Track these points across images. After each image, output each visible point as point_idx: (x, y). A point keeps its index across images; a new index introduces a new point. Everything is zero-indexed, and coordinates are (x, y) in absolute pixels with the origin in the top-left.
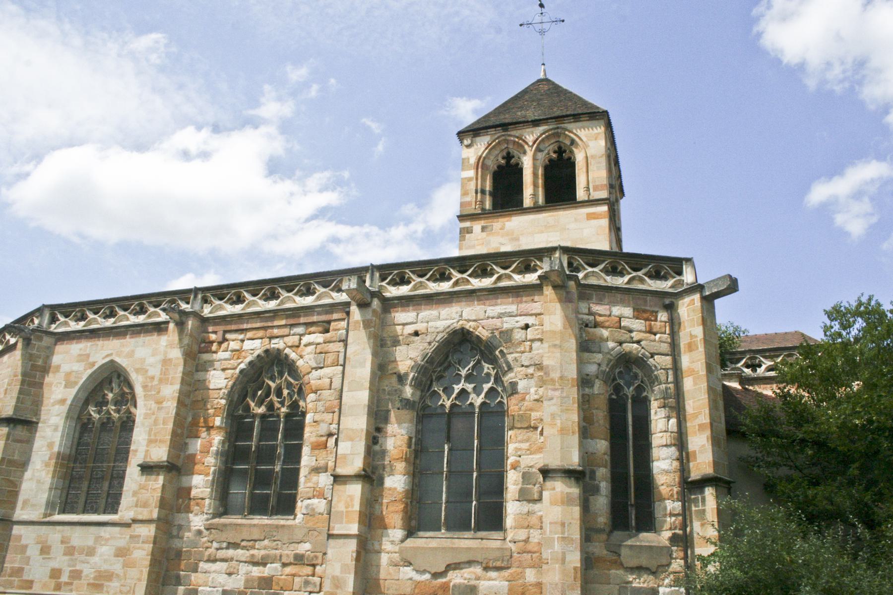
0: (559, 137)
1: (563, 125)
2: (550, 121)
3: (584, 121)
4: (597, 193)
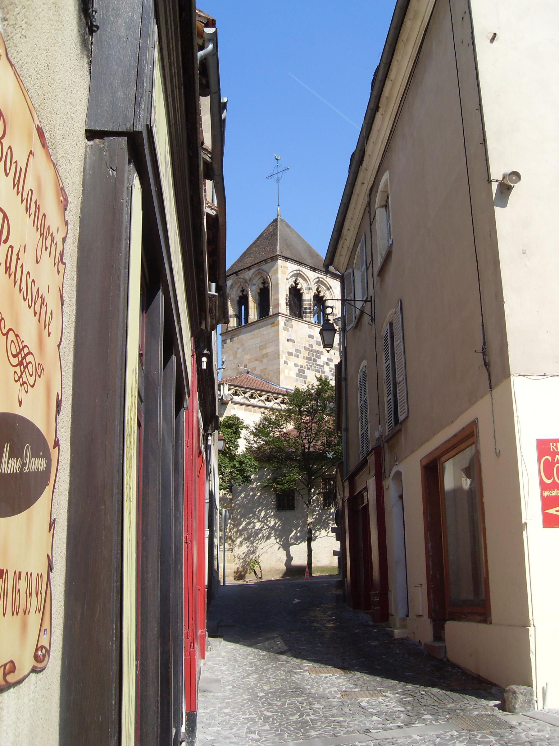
1: (261, 267)
4: (275, 309)
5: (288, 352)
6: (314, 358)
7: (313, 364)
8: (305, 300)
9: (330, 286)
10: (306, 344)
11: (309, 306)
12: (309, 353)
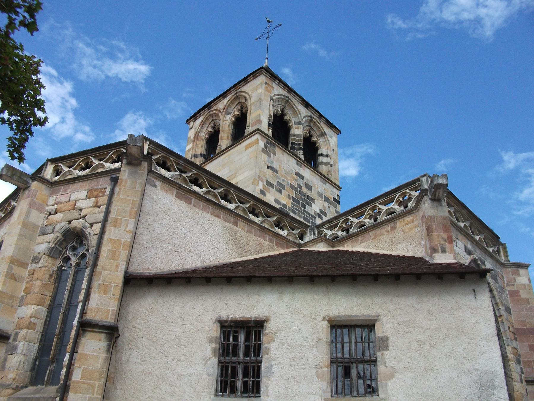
0: (239, 99)
2: (231, 90)
3: (251, 81)
4: (253, 128)
5: (267, 182)
6: (303, 202)
7: (301, 209)
8: (294, 135)
9: (325, 132)
10: (293, 182)
11: (298, 142)
12: (295, 193)
